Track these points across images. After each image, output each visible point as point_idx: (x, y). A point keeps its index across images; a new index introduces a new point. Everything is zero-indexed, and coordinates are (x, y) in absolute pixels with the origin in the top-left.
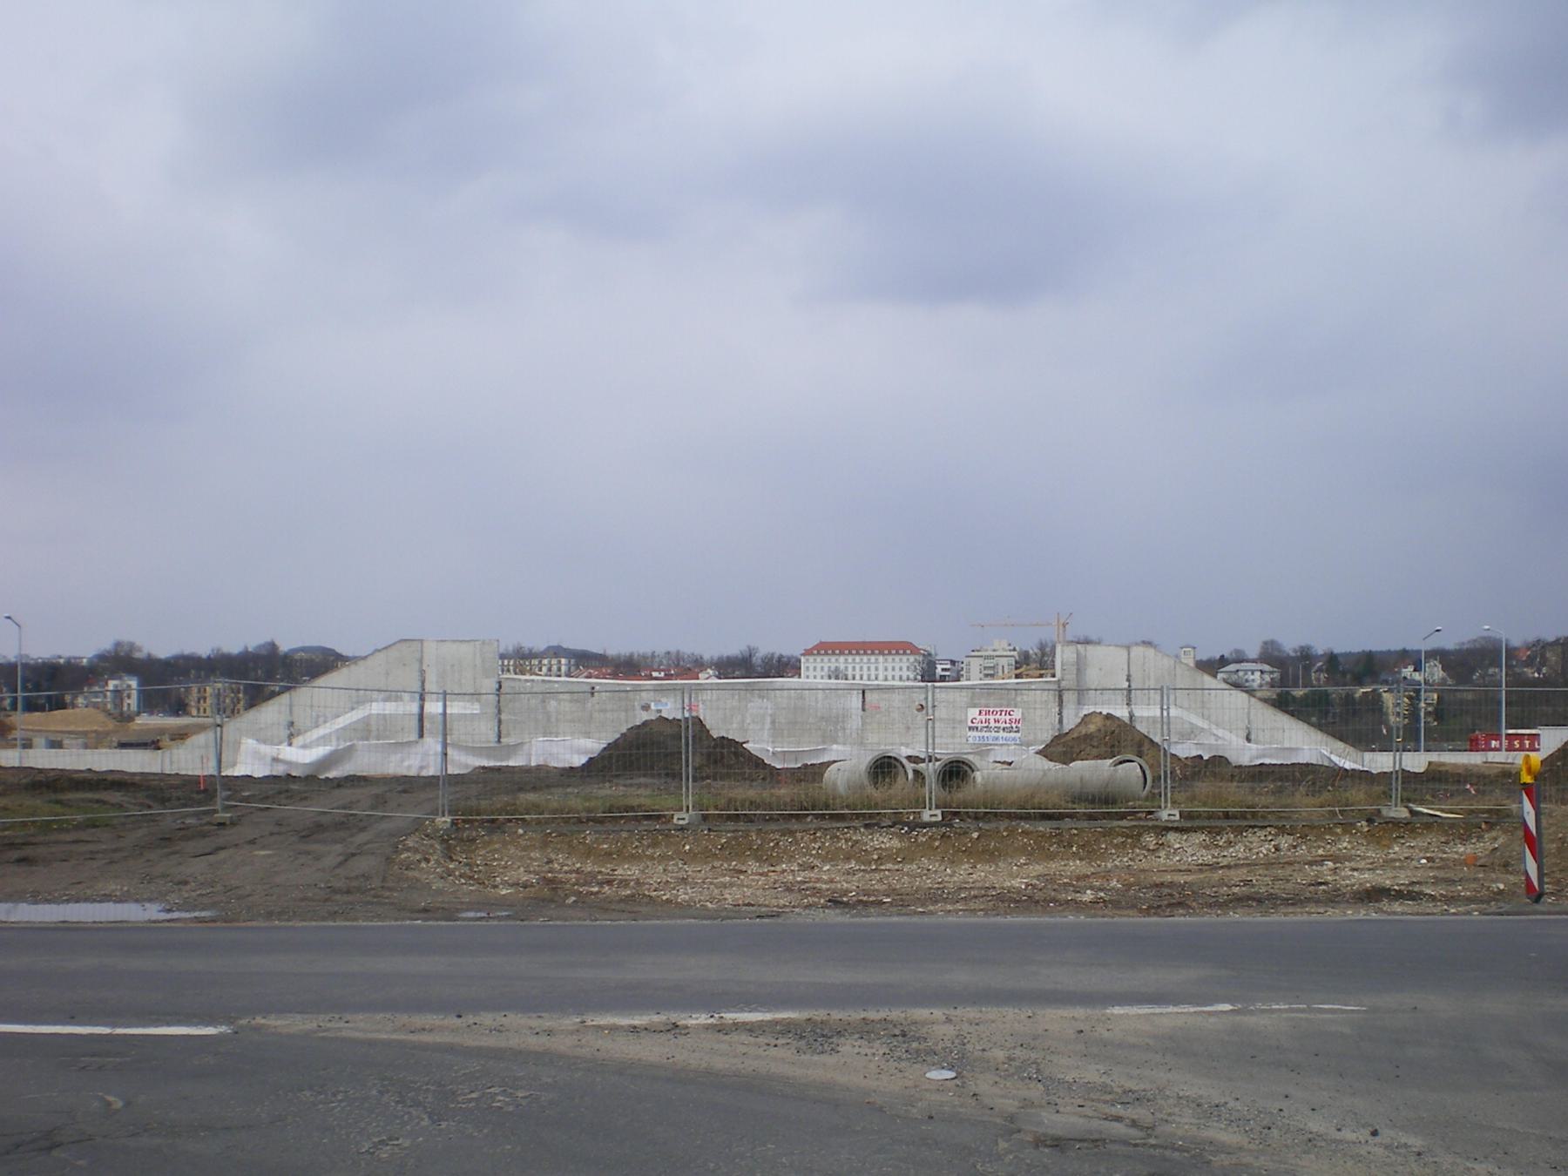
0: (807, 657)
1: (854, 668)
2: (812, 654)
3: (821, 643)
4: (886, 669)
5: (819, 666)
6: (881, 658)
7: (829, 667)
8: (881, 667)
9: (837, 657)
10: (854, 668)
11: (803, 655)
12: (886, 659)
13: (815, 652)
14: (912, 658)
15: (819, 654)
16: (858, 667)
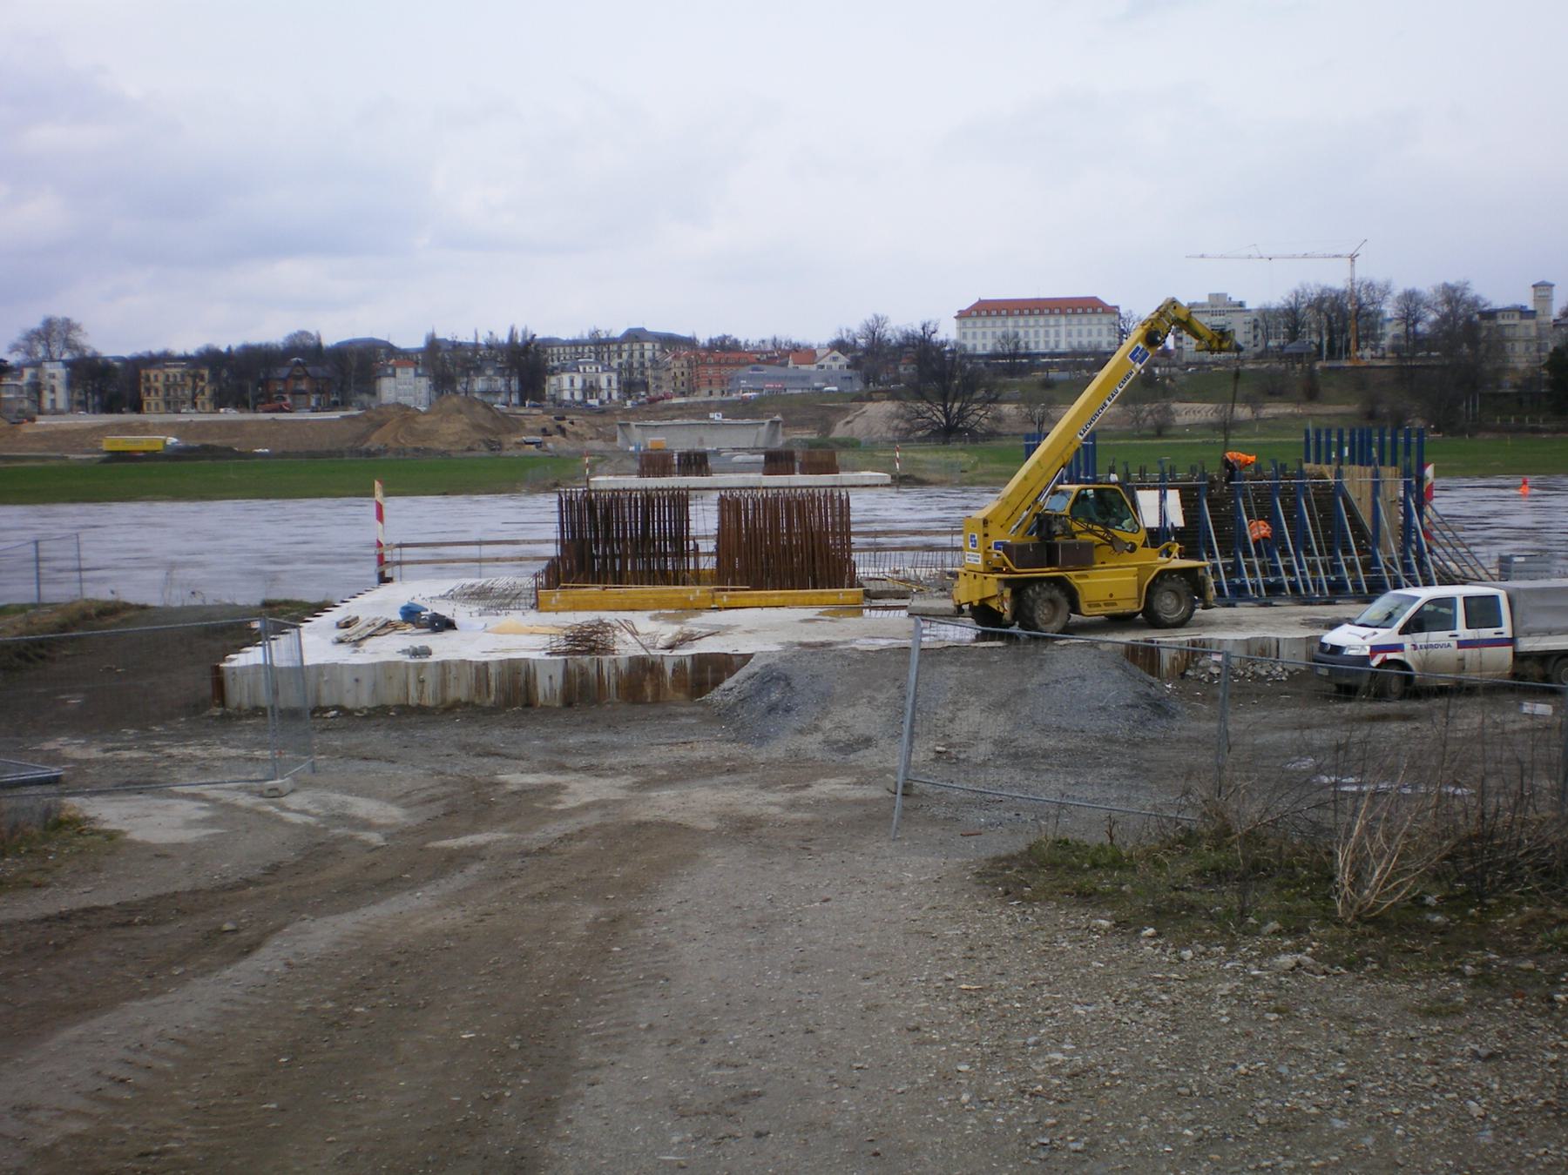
0: (963, 320)
1: (1027, 333)
4: (1069, 334)
5: (979, 332)
6: (1063, 320)
7: (994, 333)
8: (1063, 330)
9: (1003, 319)
10: (1027, 333)
13: (974, 313)
15: (979, 315)
16: (1031, 331)
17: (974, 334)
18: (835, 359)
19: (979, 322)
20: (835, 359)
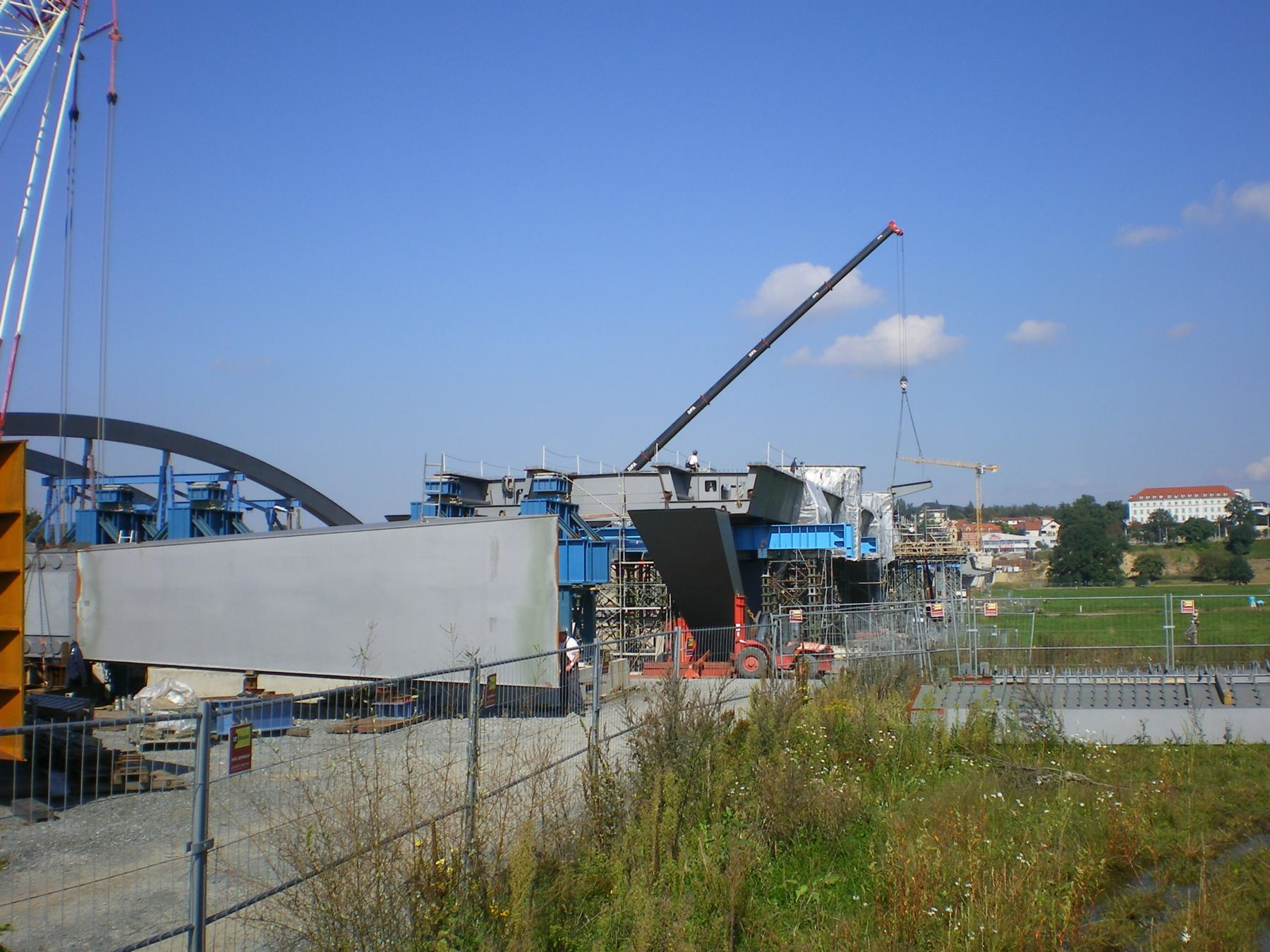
2: (1139, 500)
6: (1201, 501)
8: (1201, 508)
11: (1130, 501)
15: (1144, 499)
16: (1180, 510)
18: (1053, 527)
19: (1145, 503)
20: (1053, 527)
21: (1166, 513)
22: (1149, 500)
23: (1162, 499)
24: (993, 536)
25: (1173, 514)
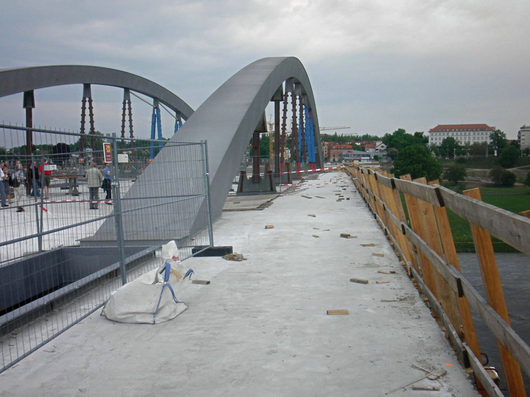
0: (432, 133)
1: (457, 138)
3: (439, 126)
6: (472, 133)
8: (472, 137)
12: (474, 134)
14: (489, 133)
15: (438, 131)
16: (459, 138)
17: (436, 139)
19: (438, 134)
20: (382, 147)
21: (452, 139)
22: (441, 131)
23: (449, 131)
24: (349, 152)
25: (455, 138)
